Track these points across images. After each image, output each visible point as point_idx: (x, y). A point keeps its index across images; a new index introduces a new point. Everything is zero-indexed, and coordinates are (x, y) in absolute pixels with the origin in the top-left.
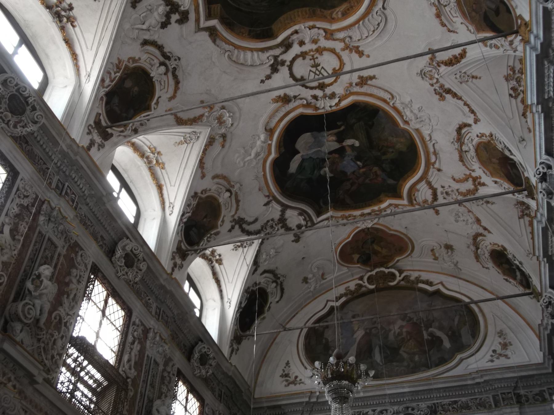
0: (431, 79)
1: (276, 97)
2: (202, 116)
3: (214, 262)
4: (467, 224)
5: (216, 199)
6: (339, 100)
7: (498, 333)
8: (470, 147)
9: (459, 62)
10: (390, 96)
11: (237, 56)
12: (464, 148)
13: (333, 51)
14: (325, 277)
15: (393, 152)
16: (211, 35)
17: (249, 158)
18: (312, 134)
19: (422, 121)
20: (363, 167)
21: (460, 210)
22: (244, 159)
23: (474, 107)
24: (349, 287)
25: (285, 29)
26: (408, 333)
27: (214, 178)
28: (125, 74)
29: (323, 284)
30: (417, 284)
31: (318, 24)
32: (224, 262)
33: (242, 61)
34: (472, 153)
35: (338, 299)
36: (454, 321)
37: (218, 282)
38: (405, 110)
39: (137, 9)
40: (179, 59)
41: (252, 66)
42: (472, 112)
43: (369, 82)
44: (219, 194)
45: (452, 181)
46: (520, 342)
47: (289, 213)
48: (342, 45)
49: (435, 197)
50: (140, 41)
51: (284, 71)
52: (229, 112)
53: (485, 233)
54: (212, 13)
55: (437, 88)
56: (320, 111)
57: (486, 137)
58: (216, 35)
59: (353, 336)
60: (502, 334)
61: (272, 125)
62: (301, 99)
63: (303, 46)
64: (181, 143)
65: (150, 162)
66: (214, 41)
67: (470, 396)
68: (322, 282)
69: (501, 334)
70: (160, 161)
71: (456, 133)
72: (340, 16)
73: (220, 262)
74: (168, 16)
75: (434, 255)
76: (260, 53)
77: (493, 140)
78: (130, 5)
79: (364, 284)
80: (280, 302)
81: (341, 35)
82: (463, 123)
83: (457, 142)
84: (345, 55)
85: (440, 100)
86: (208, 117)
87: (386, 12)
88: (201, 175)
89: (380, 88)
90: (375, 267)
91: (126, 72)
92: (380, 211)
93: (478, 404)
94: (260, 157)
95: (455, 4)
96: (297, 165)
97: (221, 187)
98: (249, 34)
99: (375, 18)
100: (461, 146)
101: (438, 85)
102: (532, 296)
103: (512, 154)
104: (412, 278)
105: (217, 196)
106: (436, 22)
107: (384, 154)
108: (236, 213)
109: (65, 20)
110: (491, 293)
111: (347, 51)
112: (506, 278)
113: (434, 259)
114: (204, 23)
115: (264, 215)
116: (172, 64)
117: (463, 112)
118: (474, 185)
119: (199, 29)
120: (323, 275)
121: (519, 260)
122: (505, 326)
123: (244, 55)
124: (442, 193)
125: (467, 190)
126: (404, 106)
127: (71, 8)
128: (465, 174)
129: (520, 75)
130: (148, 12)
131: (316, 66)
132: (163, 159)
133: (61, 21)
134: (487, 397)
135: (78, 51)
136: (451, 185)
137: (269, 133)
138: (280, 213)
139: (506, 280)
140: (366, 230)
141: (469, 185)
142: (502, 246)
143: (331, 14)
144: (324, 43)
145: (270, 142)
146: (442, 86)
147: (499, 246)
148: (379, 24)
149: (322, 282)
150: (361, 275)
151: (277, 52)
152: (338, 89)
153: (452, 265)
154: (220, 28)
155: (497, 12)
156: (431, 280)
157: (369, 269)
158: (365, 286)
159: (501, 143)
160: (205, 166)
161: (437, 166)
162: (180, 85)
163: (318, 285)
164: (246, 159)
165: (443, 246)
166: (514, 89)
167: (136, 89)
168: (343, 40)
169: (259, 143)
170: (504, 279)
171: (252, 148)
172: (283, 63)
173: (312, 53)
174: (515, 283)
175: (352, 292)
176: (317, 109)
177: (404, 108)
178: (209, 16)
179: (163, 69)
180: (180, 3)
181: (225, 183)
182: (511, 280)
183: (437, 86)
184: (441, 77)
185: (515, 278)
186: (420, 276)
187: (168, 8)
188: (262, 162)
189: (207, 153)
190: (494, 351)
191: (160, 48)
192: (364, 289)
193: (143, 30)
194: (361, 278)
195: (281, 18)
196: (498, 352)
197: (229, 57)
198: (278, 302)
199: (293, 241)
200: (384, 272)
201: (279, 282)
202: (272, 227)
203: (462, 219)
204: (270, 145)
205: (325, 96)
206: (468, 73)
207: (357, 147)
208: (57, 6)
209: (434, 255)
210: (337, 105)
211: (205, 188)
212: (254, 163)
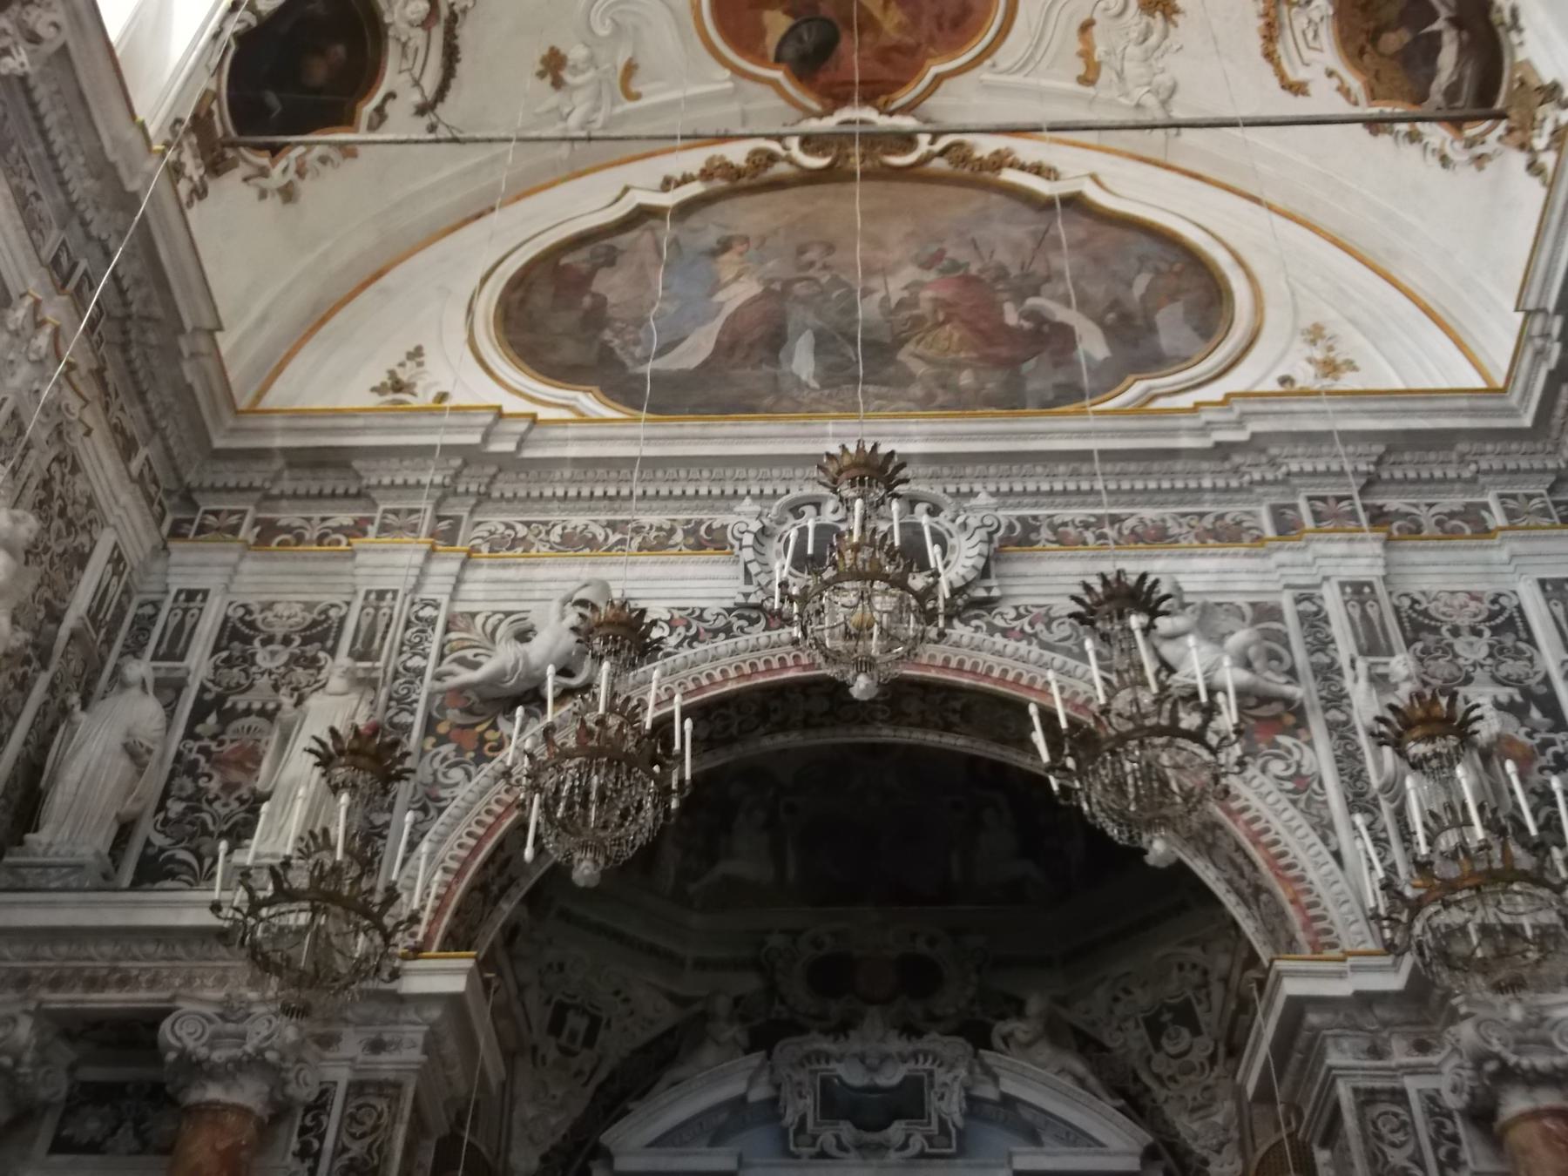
14: (635, 87)
26: (938, 303)
29: (624, 117)
36: (1130, 285)
46: (1391, 362)
59: (712, 294)
67: (1180, 503)
68: (618, 110)
90: (841, 100)
93: (1207, 530)
120: (630, 69)
134: (1248, 513)
157: (814, 105)
158: (791, 161)
163: (600, 118)
192: (781, 168)
209: (1086, 54)
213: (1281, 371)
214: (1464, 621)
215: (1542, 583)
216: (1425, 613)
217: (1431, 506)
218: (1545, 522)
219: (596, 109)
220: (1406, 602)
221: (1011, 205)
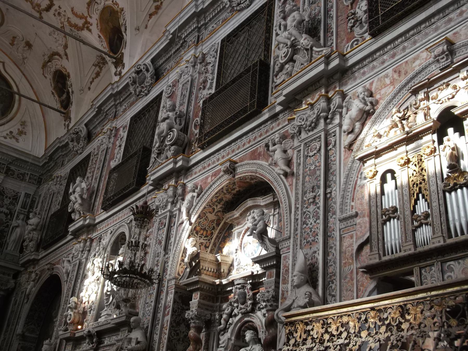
4: (56, 42)
7: (22, 122)
34: (101, 7)
45: (70, 10)
49: (48, 9)
53: (64, 57)
57: (118, 7)
60: (24, 125)
69: (23, 124)
75: (13, 41)
77: (121, 13)
102: (63, 115)
103: (125, 32)
112: (54, 92)
113: (10, 44)
122: (29, 120)
124: (56, 10)
125: (75, 24)
136: (66, 11)
139: (53, 93)
141: (80, 23)
142: (69, 73)
147: (66, 71)
153: (21, 57)
159: (124, 20)
165: (24, 41)
182: (56, 95)
185: (59, 97)
190: (11, 132)
196: (13, 134)
209: (13, 41)
213: (11, 130)
214: (9, 196)
215: (26, 193)
216: (4, 192)
217: (19, 170)
218: (34, 182)
220: (2, 188)
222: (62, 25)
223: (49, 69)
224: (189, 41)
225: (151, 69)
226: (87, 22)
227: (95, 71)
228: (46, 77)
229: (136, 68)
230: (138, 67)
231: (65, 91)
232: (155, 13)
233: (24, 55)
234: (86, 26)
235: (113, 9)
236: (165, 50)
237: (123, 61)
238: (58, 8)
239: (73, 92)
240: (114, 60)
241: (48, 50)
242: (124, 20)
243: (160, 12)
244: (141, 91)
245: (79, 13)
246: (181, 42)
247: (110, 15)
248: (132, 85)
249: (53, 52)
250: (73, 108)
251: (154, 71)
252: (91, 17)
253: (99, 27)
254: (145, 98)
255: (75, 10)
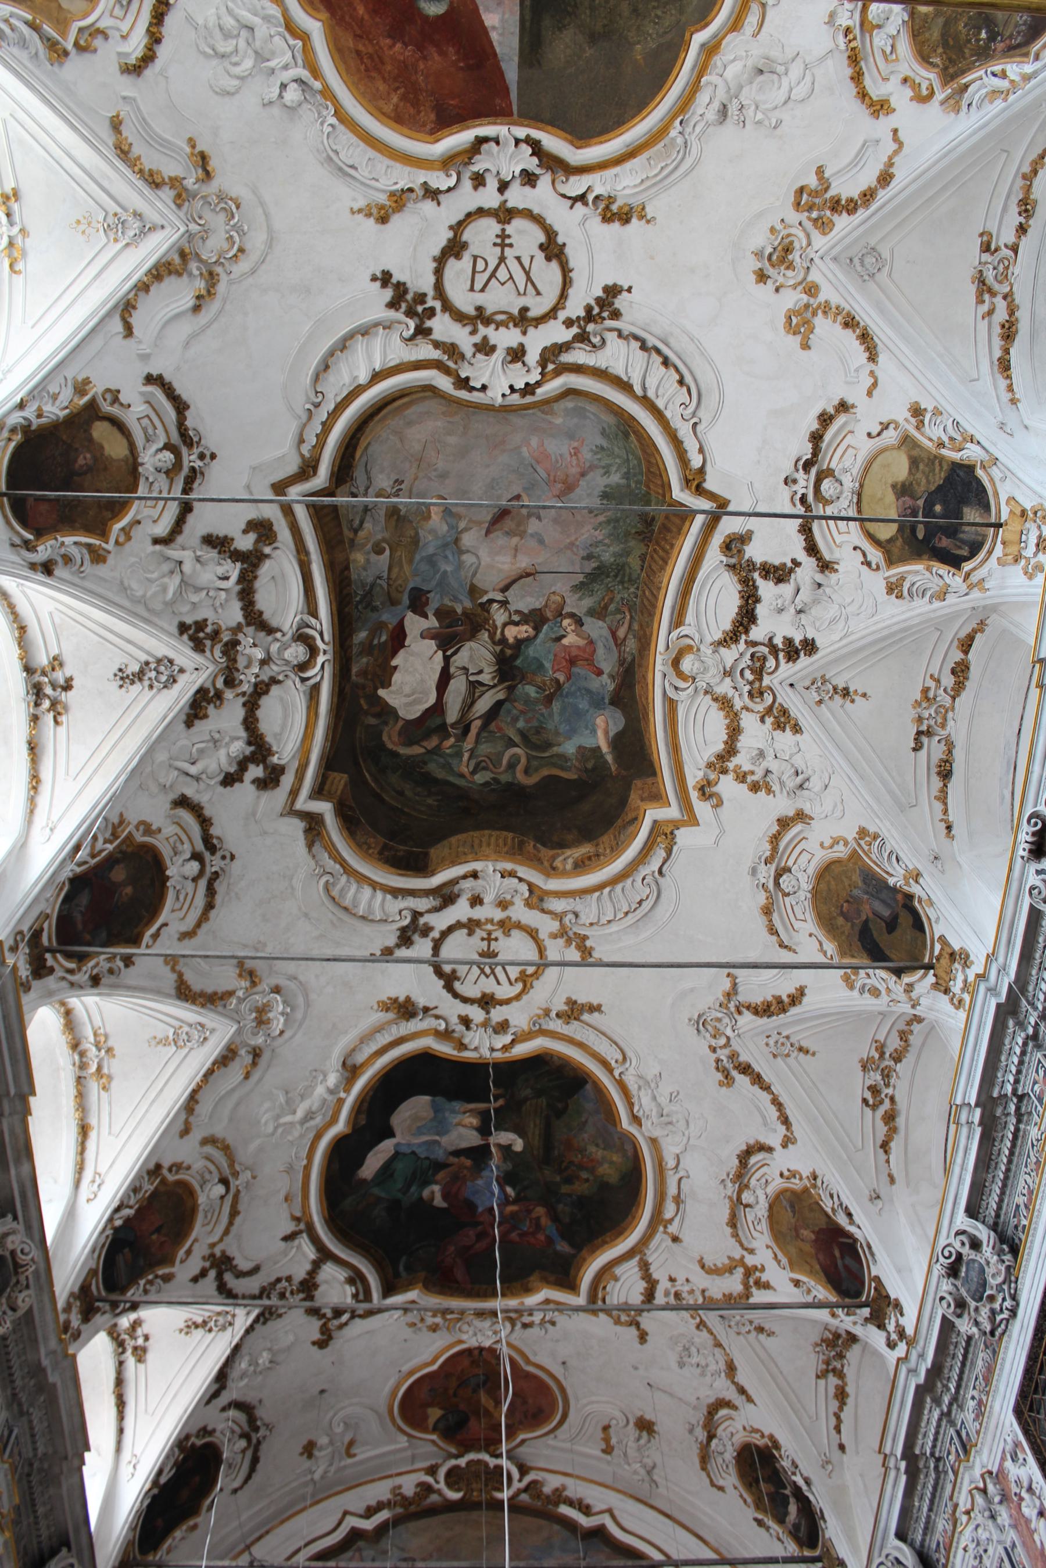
0: (715, 1037)
1: (390, 999)
2: (231, 994)
3: (129, 1352)
4: (703, 1374)
5: (191, 1192)
6: (513, 1041)
8: (759, 1198)
9: (784, 1010)
10: (620, 1057)
11: (342, 889)
12: (746, 1197)
13: (532, 933)
14: (353, 1451)
15: (587, 1180)
16: (308, 831)
17: (288, 1118)
18: (433, 1101)
19: (670, 1123)
20: (515, 1201)
21: (697, 1340)
22: (278, 1117)
23: (791, 1111)
24: (400, 1487)
25: (454, 863)
27: (205, 1141)
28: (121, 852)
29: (345, 1467)
30: (557, 1504)
31: (523, 871)
32: (150, 1356)
33: (347, 902)
34: (762, 1210)
35: (370, 1512)
37: (121, 1404)
38: (642, 1093)
39: (193, 730)
40: (233, 857)
41: (363, 918)
42: (786, 1121)
43: (586, 1017)
44: (203, 1183)
47: (330, 1272)
48: (554, 926)
50: (173, 796)
51: (422, 947)
52: (284, 1002)
54: (326, 787)
55: (722, 1057)
56: (468, 1055)
57: (801, 1179)
58: (319, 834)
61: (360, 1058)
62: (437, 1017)
63: (478, 907)
64: (164, 1042)
65: (83, 1066)
66: (310, 846)
68: (343, 1463)
70: (105, 1071)
71: (737, 1162)
72: (569, 866)
73: (140, 1354)
74: (243, 765)
75: (607, 1440)
76: (389, 897)
77: (815, 1186)
78: (184, 717)
79: (436, 1486)
80: (239, 1493)
81: (558, 905)
82: (757, 1142)
83: (733, 1182)
84: (555, 950)
85: (721, 1084)
86: (241, 1001)
87: (661, 880)
88: (182, 1127)
89: (604, 1034)
91: (124, 847)
92: (519, 1312)
94: (312, 1123)
95: (809, 895)
96: (381, 1162)
97: (212, 1168)
98: (380, 853)
99: (635, 889)
100: (740, 1193)
101: (726, 1051)
104: (547, 1490)
105: (197, 1187)
106: (761, 921)
107: (569, 1180)
108: (221, 1240)
109: (46, 704)
110: (715, 1551)
111: (561, 942)
112: (760, 1517)
113: (604, 1451)
114: (303, 803)
115: (275, 1263)
116: (214, 863)
117: (764, 1117)
118: (746, 1286)
119: (291, 811)
120: (351, 1443)
121: (806, 1474)
123: (357, 891)
126: (641, 1083)
127: (67, 687)
128: (729, 1258)
129: (892, 1063)
130: (211, 745)
131: (490, 954)
132: (113, 1067)
133: (37, 705)
135: (46, 774)
137: (346, 1074)
138: (308, 1267)
139: (760, 1523)
140: (476, 1352)
141: (734, 1284)
142: (771, 1437)
143: (554, 858)
144: (519, 912)
145: (343, 1095)
146: (733, 1056)
147: (763, 1436)
148: (640, 903)
149: (343, 1463)
150: (434, 1462)
151: (422, 904)
152: (519, 1016)
153: (643, 1472)
154: (331, 821)
155: (892, 925)
156: (588, 1501)
157: (453, 1450)
158: (439, 1492)
159: (832, 1196)
160: (198, 1108)
161: (673, 1229)
162: (213, 914)
163: (333, 1469)
164: (283, 1120)
166: (874, 1090)
167: (129, 890)
168: (559, 917)
169: (320, 1090)
170: (756, 1519)
171: (303, 1097)
172: (426, 931)
173: (489, 927)
174: (780, 1531)
175: (405, 1501)
176: (462, 1046)
177: (640, 1088)
178: (319, 792)
179: (195, 866)
180: (275, 749)
181: (224, 1163)
182: (770, 1522)
183: (723, 1054)
184: (739, 1035)
185: (781, 1521)
186: (564, 1488)
187: (249, 750)
188: (311, 1135)
189: (211, 1079)
191: (205, 822)
192: (434, 1498)
193: (187, 774)
194: (432, 1471)
195: (453, 840)
197: (327, 888)
198: (235, 1491)
199: (314, 1343)
200: (486, 1464)
201: (254, 1437)
202: (282, 1296)
203: (694, 1360)
204: (341, 1102)
205: (485, 1024)
206: (793, 1040)
207: (517, 1153)
208: (44, 673)
209: (607, 1440)
210: (505, 1048)
211: (179, 1160)
212: (297, 1132)
219: (331, 1465)
221: (566, 1533)
222: (698, 1320)
223: (720, 1460)
224: (1028, 1089)
225: (983, 1233)
226: (749, 1272)
227: (832, 1391)
228: (721, 1489)
229: (942, 1259)
230: (946, 1254)
231: (787, 1492)
232: (893, 1131)
233: (646, 1460)
234: (751, 1281)
235: (793, 1192)
236: (985, 1162)
237: (888, 1297)
238: (669, 1284)
239: (807, 1482)
240: (866, 1312)
241: (695, 1408)
242: (832, 1196)
243: (900, 1121)
244: (993, 1312)
245: (722, 1261)
246: (1012, 1108)
247: (794, 1212)
248: (959, 1316)
249: (709, 1406)
250: (832, 1529)
251: (992, 1234)
252: (751, 1251)
253: (784, 1261)
254: (1016, 1326)
255: (709, 1262)
